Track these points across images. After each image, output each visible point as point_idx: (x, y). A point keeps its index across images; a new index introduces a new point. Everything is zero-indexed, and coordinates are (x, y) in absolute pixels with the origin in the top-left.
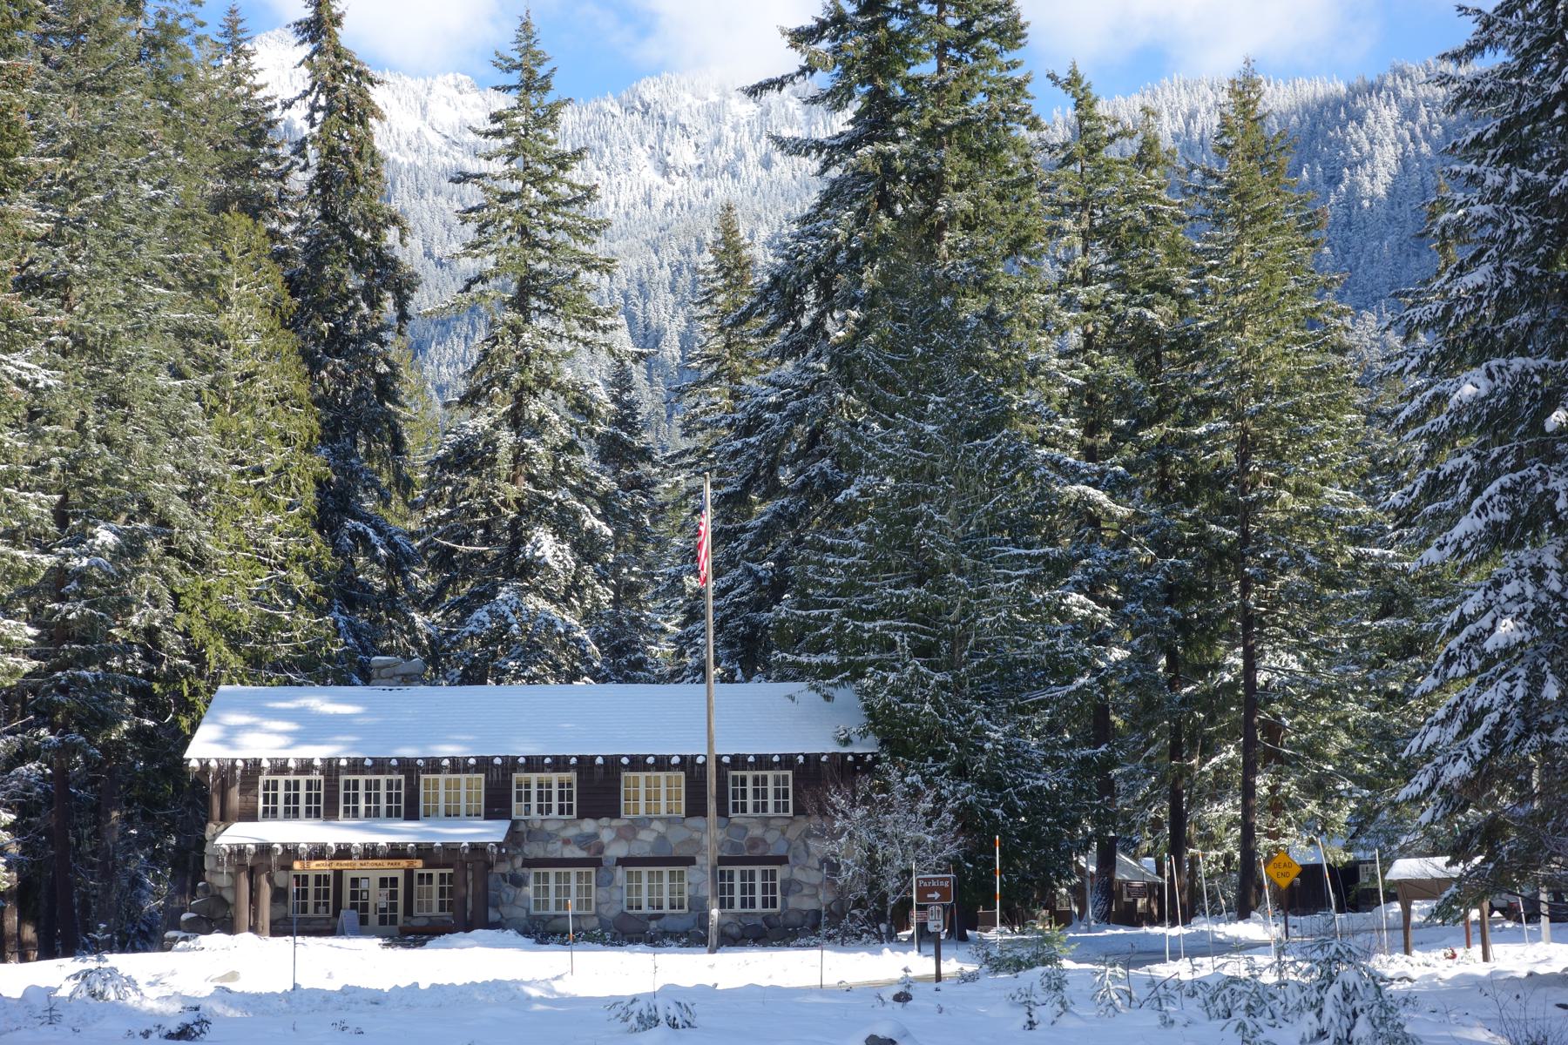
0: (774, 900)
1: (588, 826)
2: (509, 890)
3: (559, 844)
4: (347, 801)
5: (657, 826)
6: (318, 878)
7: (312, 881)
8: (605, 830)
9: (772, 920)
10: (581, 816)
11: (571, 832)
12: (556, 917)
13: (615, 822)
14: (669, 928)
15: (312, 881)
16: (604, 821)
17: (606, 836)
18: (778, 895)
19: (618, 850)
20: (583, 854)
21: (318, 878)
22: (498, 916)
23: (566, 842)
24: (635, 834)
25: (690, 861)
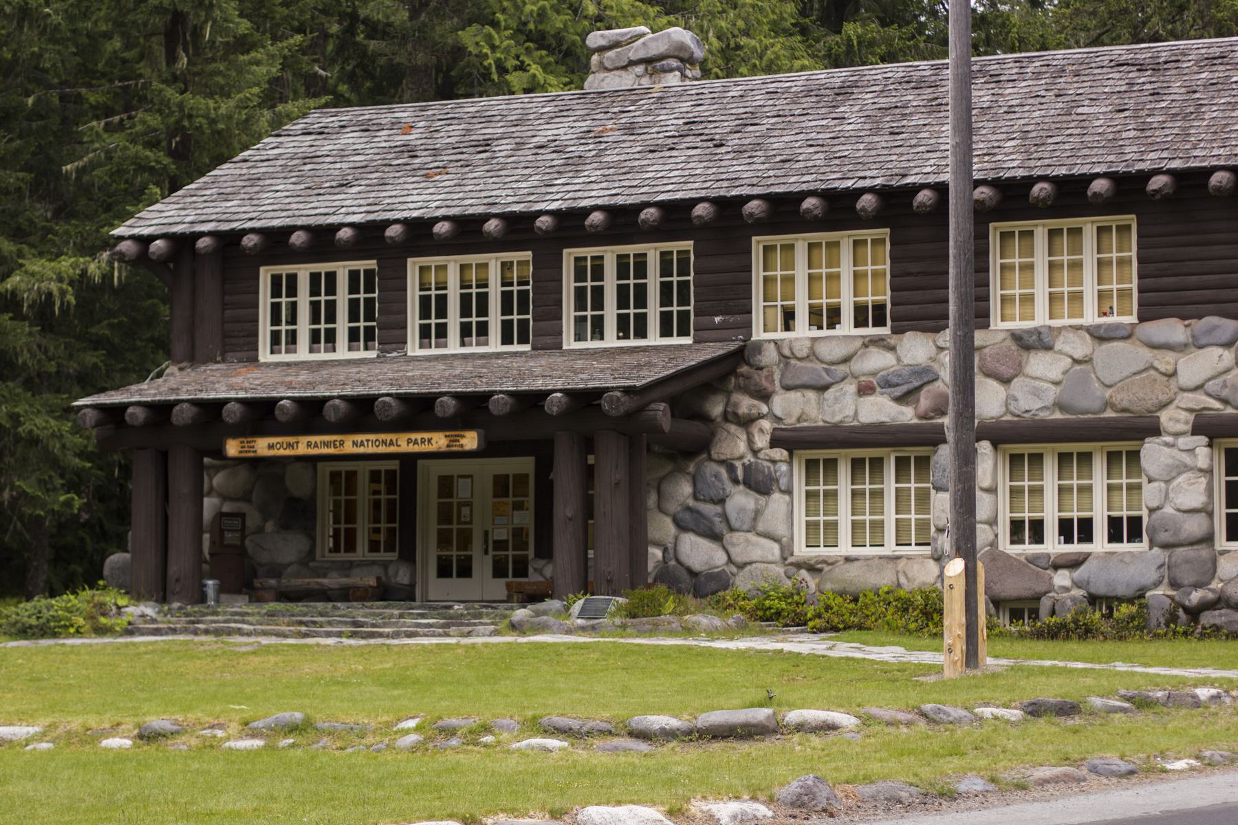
2: (741, 501)
3: (851, 388)
4: (580, 304)
5: (1080, 346)
6: (375, 476)
7: (363, 483)
11: (878, 360)
12: (848, 559)
14: (1100, 589)
20: (907, 415)
22: (719, 558)
23: (865, 390)
24: (1019, 371)
25: (1155, 430)
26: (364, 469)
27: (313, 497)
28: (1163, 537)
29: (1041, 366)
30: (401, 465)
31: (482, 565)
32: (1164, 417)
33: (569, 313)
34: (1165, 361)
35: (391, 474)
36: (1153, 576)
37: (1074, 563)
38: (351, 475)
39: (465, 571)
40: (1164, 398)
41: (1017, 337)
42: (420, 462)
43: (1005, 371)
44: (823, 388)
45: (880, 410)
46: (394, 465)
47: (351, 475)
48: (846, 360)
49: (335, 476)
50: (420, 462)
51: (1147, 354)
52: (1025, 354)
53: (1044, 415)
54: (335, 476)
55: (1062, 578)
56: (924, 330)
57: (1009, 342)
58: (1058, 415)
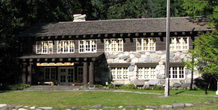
0: (183, 76)
1: (127, 54)
3: (118, 59)
6: (52, 69)
7: (50, 70)
8: (131, 54)
9: (183, 82)
10: (125, 51)
11: (121, 55)
13: (134, 52)
14: (151, 84)
15: (50, 70)
16: (131, 52)
17: (132, 56)
18: (184, 74)
19: (135, 61)
20: (125, 62)
21: (52, 69)
23: (120, 59)
25: (158, 64)
26: (51, 68)
27: (44, 72)
28: (159, 78)
29: (143, 56)
30: (56, 68)
31: (67, 80)
32: (159, 63)
33: (79, 48)
34: (159, 56)
35: (54, 69)
36: (157, 82)
37: (148, 81)
38: (49, 69)
39: (64, 81)
40: (159, 60)
41: (140, 52)
42: (59, 67)
43: (139, 57)
44: (114, 58)
45: (122, 61)
46: (55, 67)
47: (49, 69)
48: (117, 55)
49: (46, 69)
50: (59, 67)
51: (157, 55)
52: (141, 55)
53: (144, 62)
54: (46, 69)
55: (146, 83)
56: (128, 51)
57: (140, 53)
58: (145, 62)
